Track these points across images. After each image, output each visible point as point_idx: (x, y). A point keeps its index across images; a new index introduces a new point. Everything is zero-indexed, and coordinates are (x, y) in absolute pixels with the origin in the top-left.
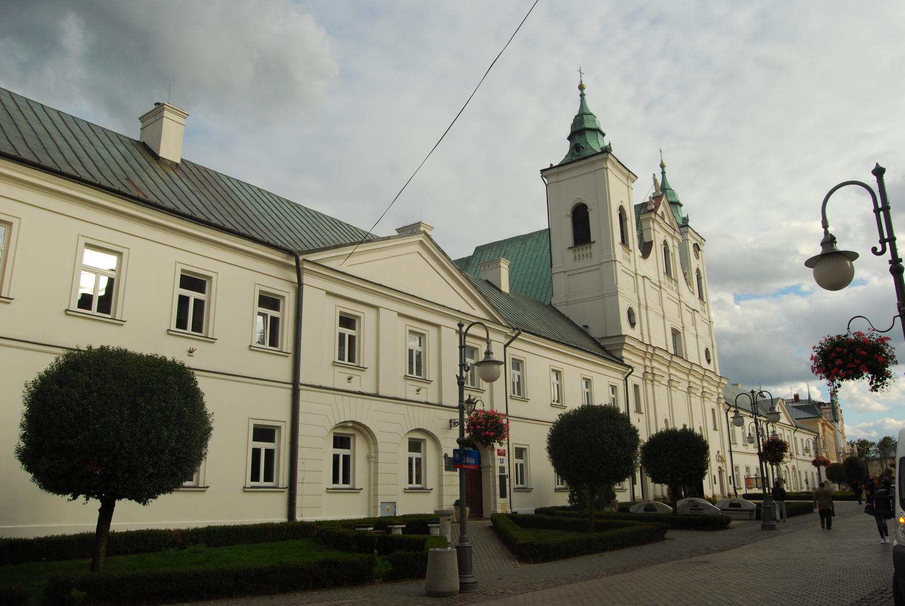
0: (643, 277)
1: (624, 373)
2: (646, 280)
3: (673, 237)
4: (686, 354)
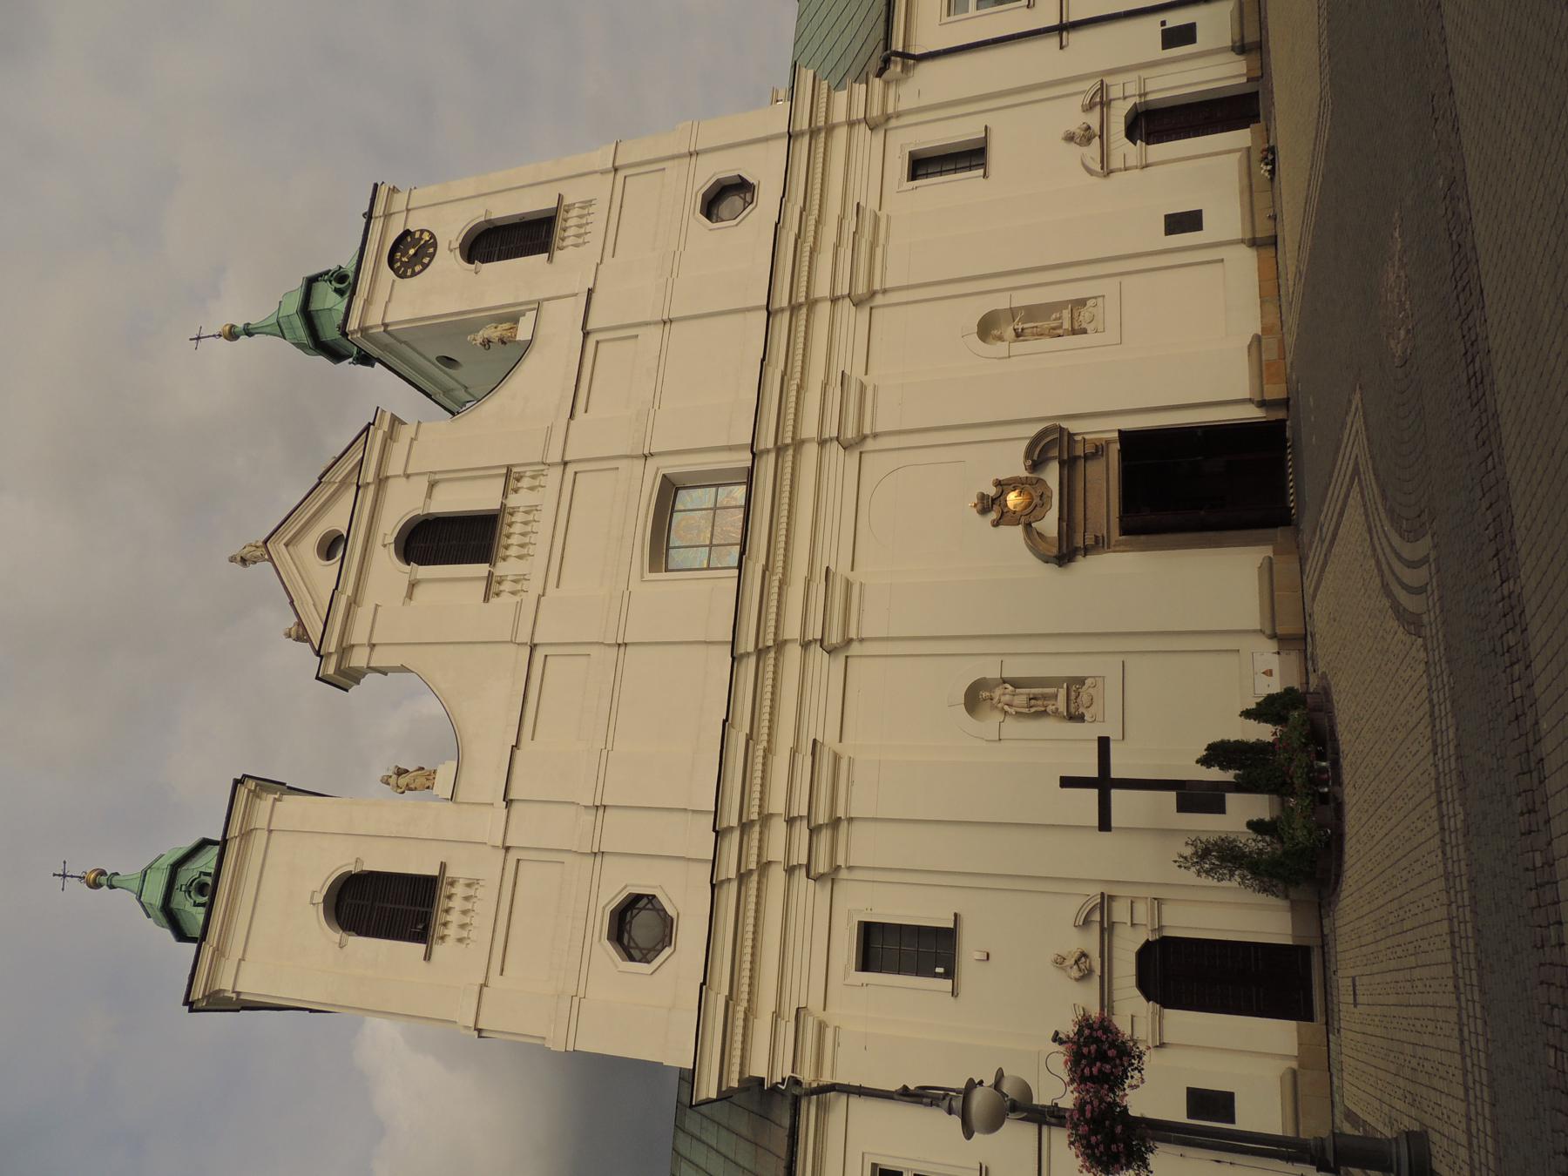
0: (508, 802)
1: (823, 1109)
2: (511, 796)
3: (381, 481)
4: (730, 448)
